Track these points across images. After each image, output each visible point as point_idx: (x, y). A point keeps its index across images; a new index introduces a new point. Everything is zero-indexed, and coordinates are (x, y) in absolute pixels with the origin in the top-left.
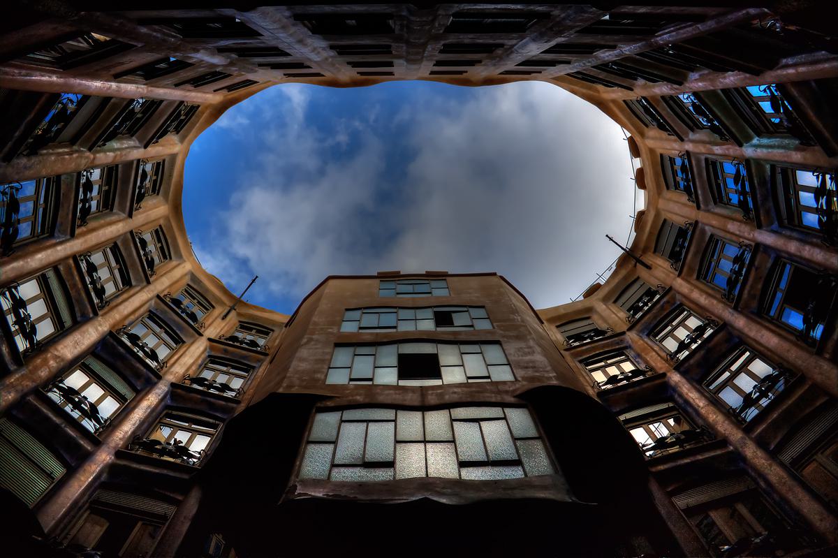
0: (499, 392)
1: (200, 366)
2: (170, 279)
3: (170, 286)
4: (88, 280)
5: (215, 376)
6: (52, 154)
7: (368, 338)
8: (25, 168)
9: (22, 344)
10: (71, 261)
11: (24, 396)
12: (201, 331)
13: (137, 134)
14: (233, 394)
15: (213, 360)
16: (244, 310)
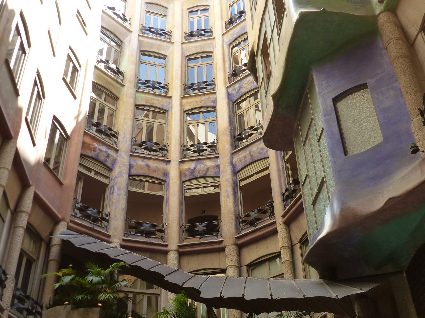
3: (222, 18)
8: (124, 137)
10: (184, 101)
11: (232, 163)
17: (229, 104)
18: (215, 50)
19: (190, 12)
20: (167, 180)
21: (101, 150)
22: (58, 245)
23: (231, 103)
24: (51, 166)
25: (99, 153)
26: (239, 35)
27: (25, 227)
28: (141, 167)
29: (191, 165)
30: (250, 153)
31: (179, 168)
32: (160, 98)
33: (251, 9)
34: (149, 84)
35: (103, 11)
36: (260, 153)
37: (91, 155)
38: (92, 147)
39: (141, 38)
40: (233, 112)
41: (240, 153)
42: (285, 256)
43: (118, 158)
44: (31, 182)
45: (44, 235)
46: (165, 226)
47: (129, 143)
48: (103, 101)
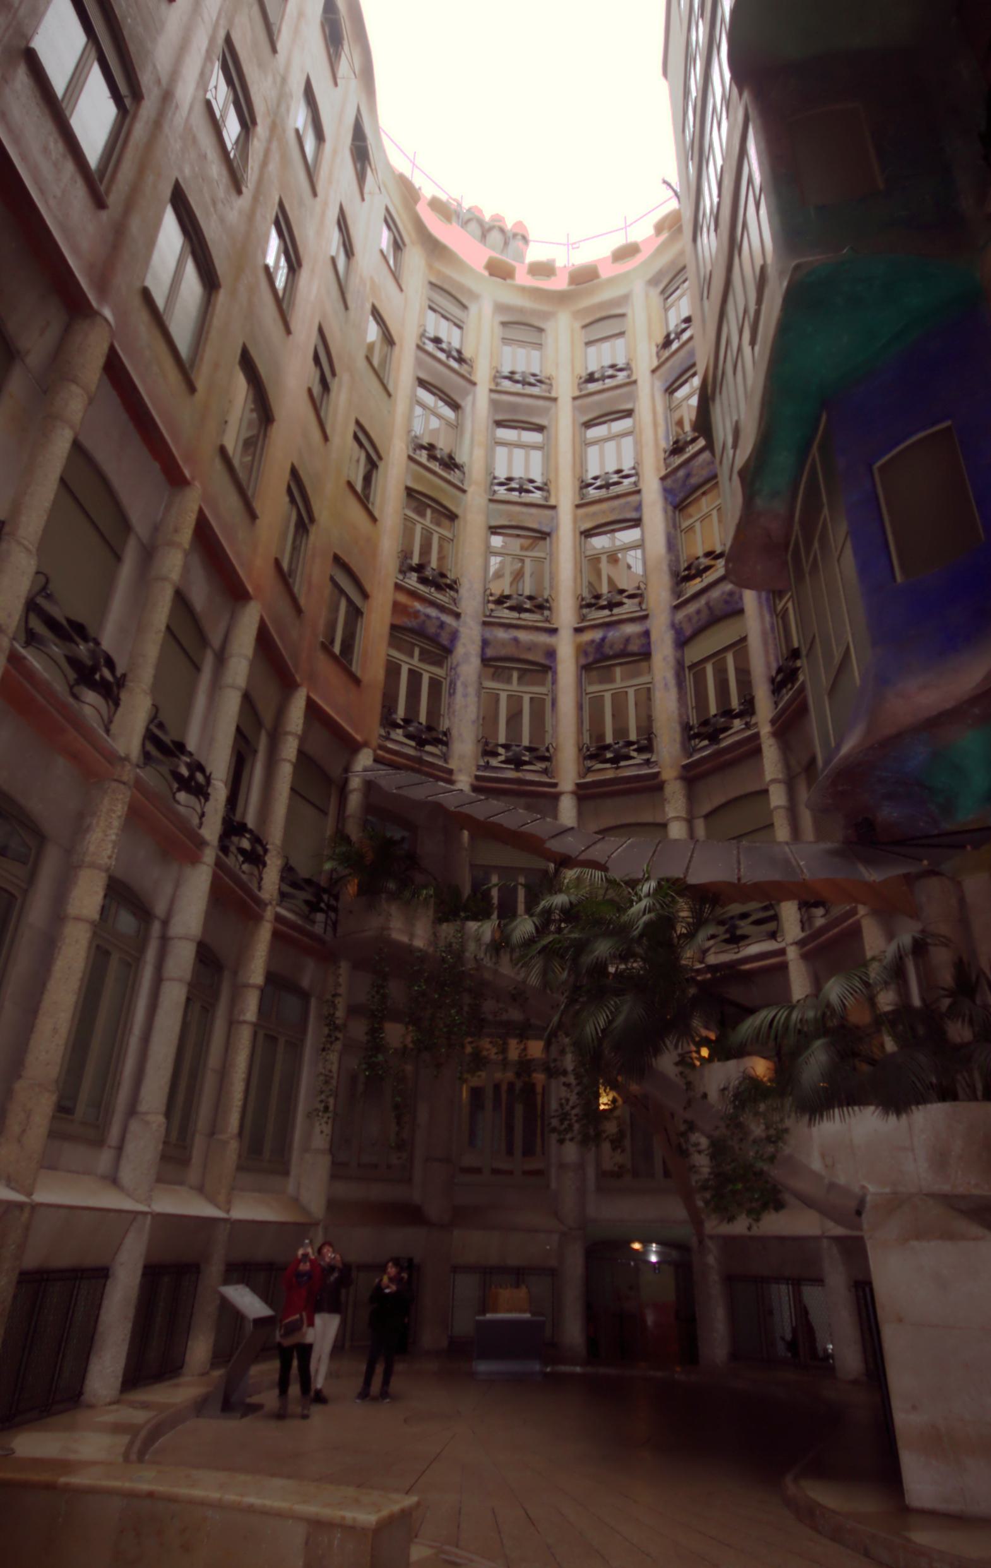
3: (650, 337)
11: (673, 625)
17: (666, 511)
21: (428, 616)
23: (670, 508)
24: (337, 649)
25: (424, 622)
27: (294, 760)
28: (503, 644)
29: (597, 635)
30: (707, 604)
32: (533, 511)
33: (702, 299)
34: (514, 485)
35: (419, 347)
36: (726, 602)
38: (411, 610)
39: (495, 396)
40: (674, 526)
41: (689, 606)
42: (777, 797)
43: (461, 629)
44: (298, 679)
45: (336, 772)
46: (552, 750)
47: (479, 598)
48: (427, 521)
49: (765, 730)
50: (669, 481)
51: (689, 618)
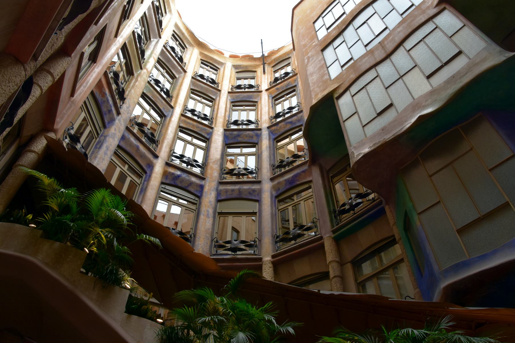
0: (424, 12)
1: (272, 106)
2: (227, 80)
4: (195, 118)
5: (283, 106)
6: (130, 90)
7: (335, 33)
9: (197, 170)
10: (183, 118)
11: (217, 190)
12: (260, 90)
13: (151, 37)
14: (297, 108)
15: (276, 99)
16: (269, 60)
18: (218, 99)
19: (202, 63)
20: (148, 172)
21: (108, 100)
22: (38, 154)
25: (104, 102)
26: (243, 99)
28: (131, 144)
29: (178, 173)
30: (239, 190)
31: (164, 168)
32: (164, 102)
36: (250, 193)
37: (98, 97)
41: (228, 185)
43: (117, 121)
49: (267, 258)
50: (228, 133)
51: (227, 191)
